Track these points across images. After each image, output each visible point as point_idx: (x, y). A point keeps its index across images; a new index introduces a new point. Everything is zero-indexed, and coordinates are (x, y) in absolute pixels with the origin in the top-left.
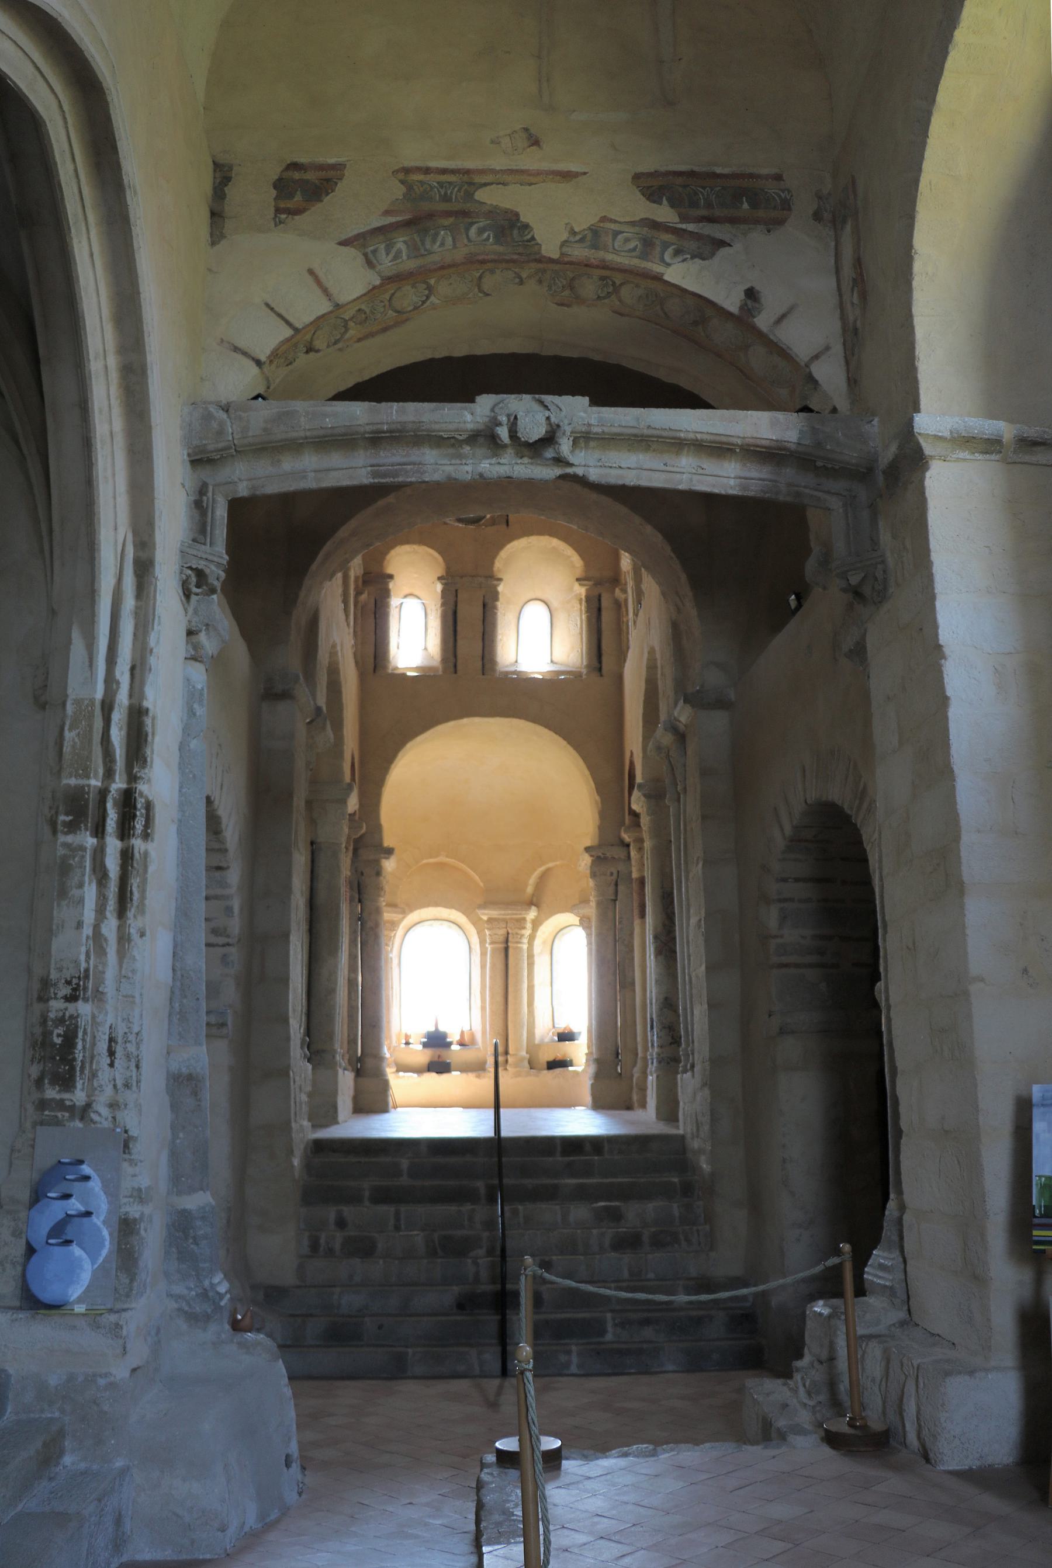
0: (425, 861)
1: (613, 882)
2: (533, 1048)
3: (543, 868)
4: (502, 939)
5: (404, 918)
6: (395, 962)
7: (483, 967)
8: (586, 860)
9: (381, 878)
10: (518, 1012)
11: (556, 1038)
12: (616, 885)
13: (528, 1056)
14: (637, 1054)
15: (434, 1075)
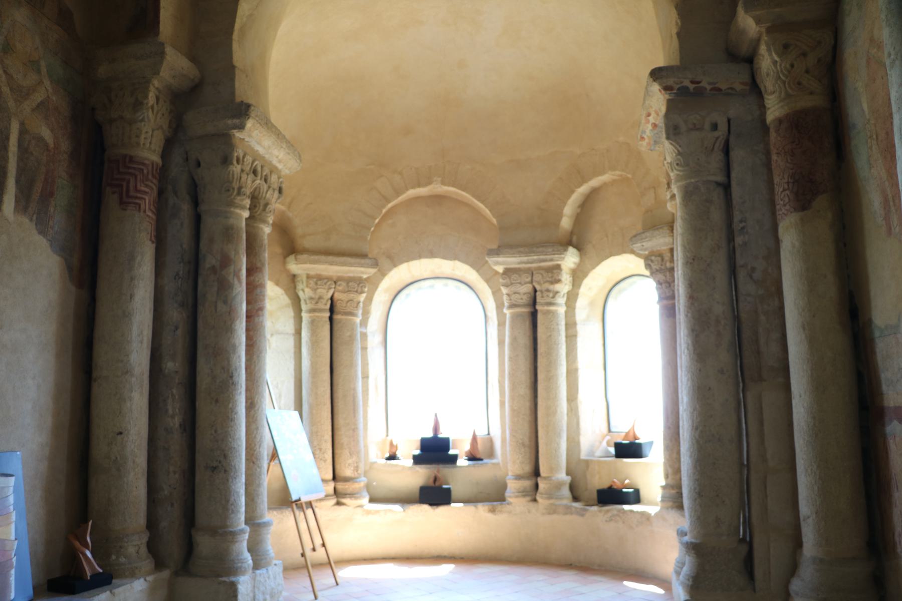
0: (412, 193)
1: (720, 145)
2: (578, 470)
3: (583, 189)
4: (526, 299)
5: (383, 274)
6: (374, 340)
7: (501, 343)
8: (658, 101)
9: (236, 168)
10: (552, 411)
11: (612, 450)
12: (727, 151)
13: (568, 479)
14: (798, 543)
15: (426, 507)
